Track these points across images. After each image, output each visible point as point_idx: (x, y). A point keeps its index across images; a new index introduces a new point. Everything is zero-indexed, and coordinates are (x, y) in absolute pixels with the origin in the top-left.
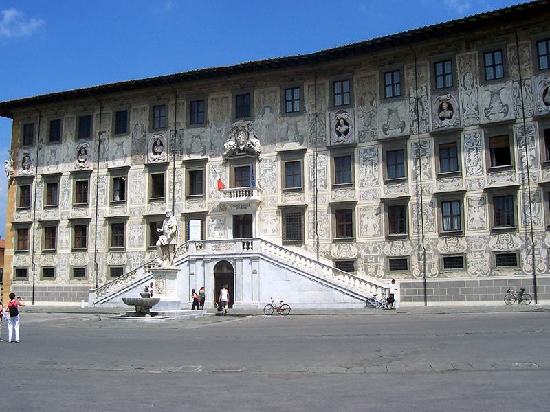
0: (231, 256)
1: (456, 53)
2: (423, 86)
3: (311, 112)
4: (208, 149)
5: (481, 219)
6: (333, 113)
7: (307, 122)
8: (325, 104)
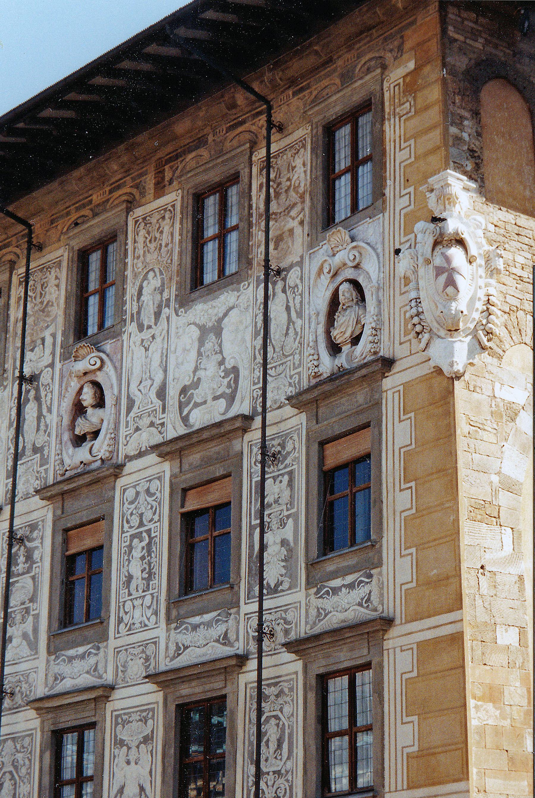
1: (128, 210)
2: (47, 334)
5: (142, 789)
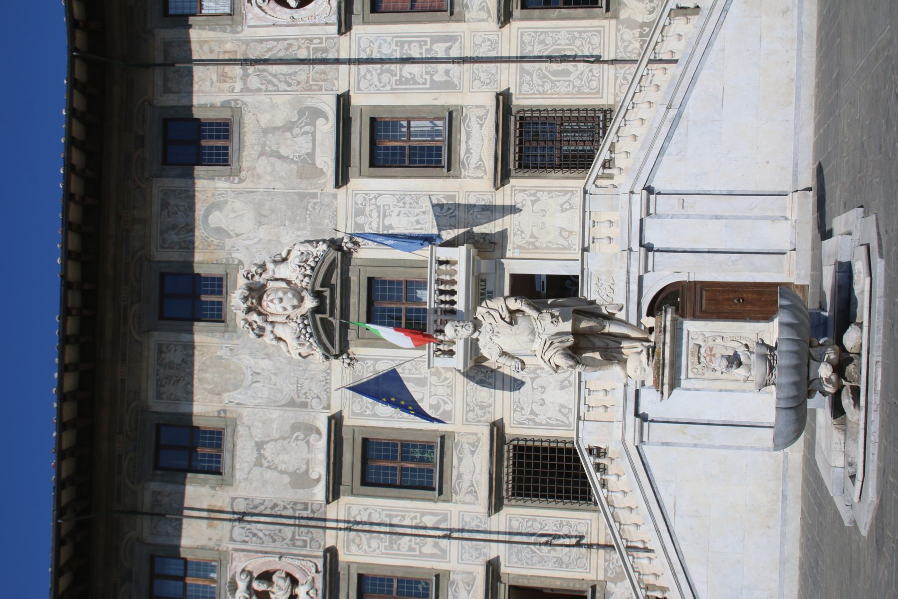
0: (634, 287)
3: (238, 86)
4: (303, 416)
6: (250, 16)
7: (262, 97)
8: (221, 42)
